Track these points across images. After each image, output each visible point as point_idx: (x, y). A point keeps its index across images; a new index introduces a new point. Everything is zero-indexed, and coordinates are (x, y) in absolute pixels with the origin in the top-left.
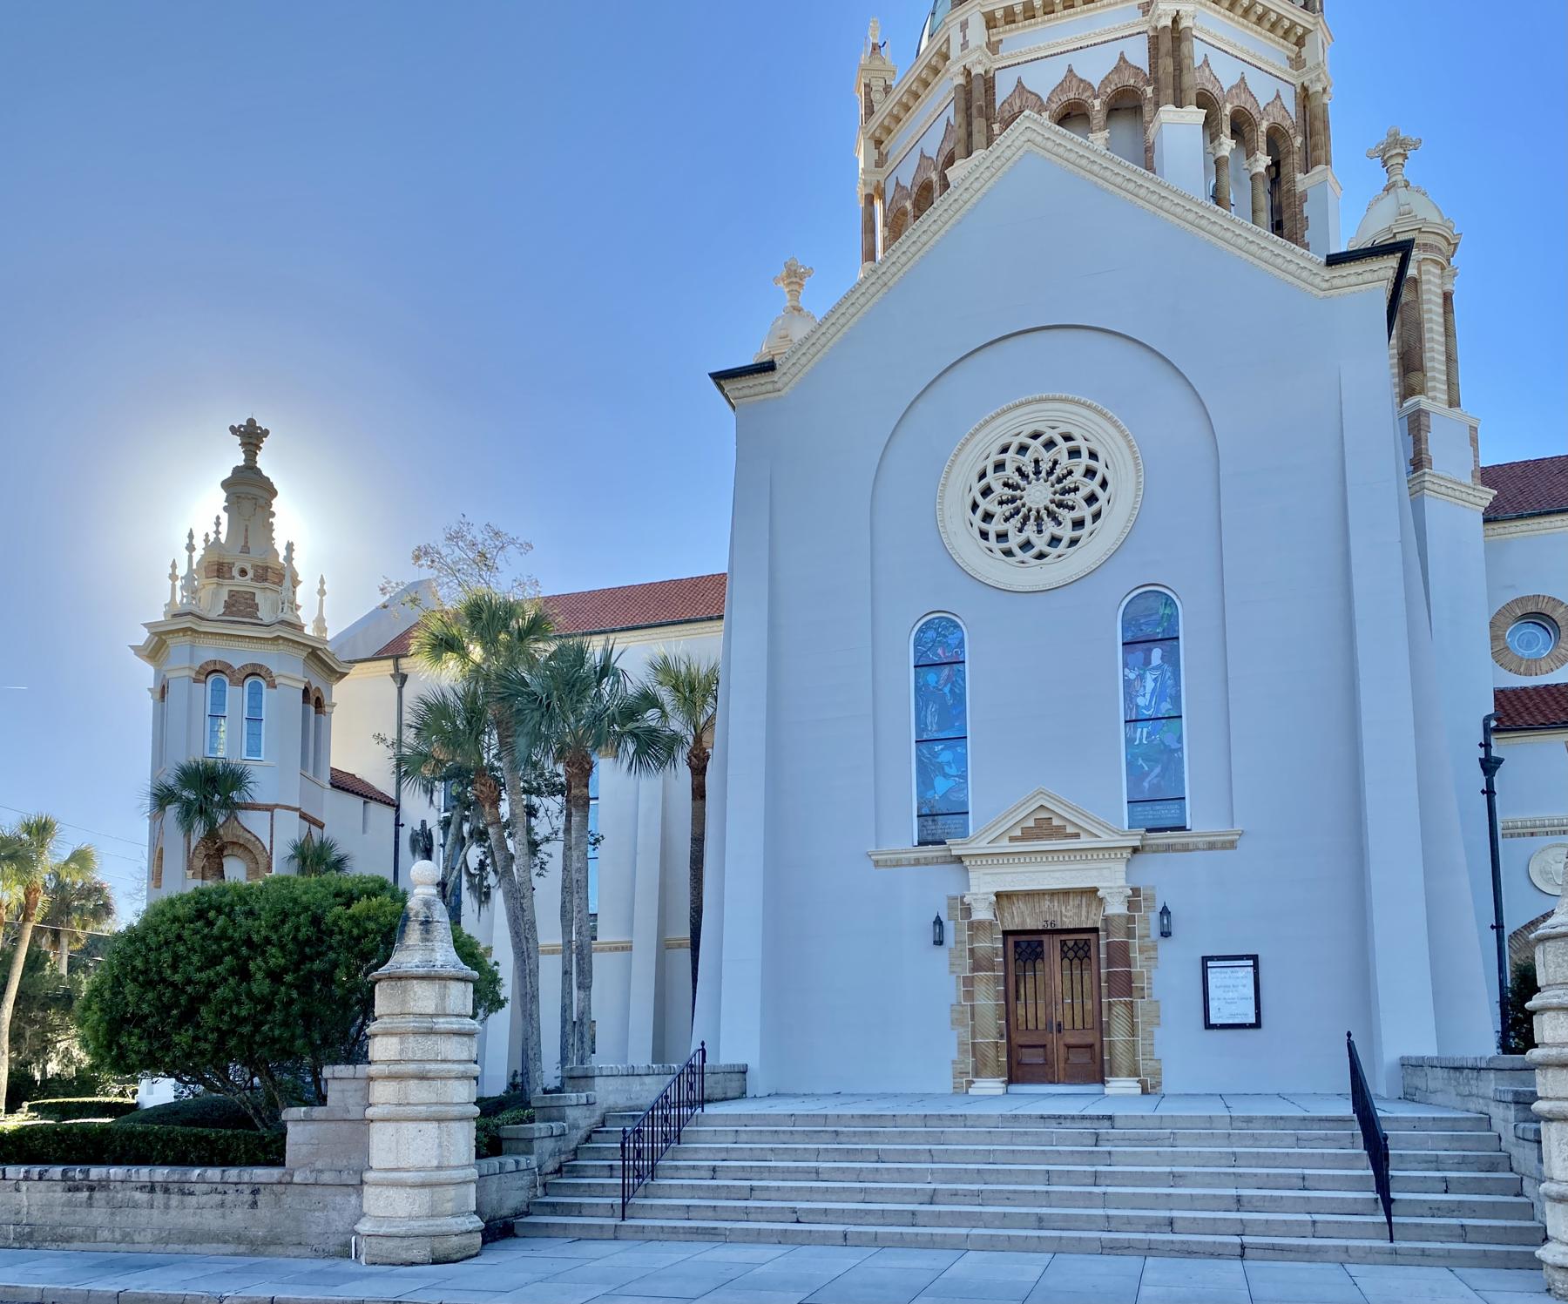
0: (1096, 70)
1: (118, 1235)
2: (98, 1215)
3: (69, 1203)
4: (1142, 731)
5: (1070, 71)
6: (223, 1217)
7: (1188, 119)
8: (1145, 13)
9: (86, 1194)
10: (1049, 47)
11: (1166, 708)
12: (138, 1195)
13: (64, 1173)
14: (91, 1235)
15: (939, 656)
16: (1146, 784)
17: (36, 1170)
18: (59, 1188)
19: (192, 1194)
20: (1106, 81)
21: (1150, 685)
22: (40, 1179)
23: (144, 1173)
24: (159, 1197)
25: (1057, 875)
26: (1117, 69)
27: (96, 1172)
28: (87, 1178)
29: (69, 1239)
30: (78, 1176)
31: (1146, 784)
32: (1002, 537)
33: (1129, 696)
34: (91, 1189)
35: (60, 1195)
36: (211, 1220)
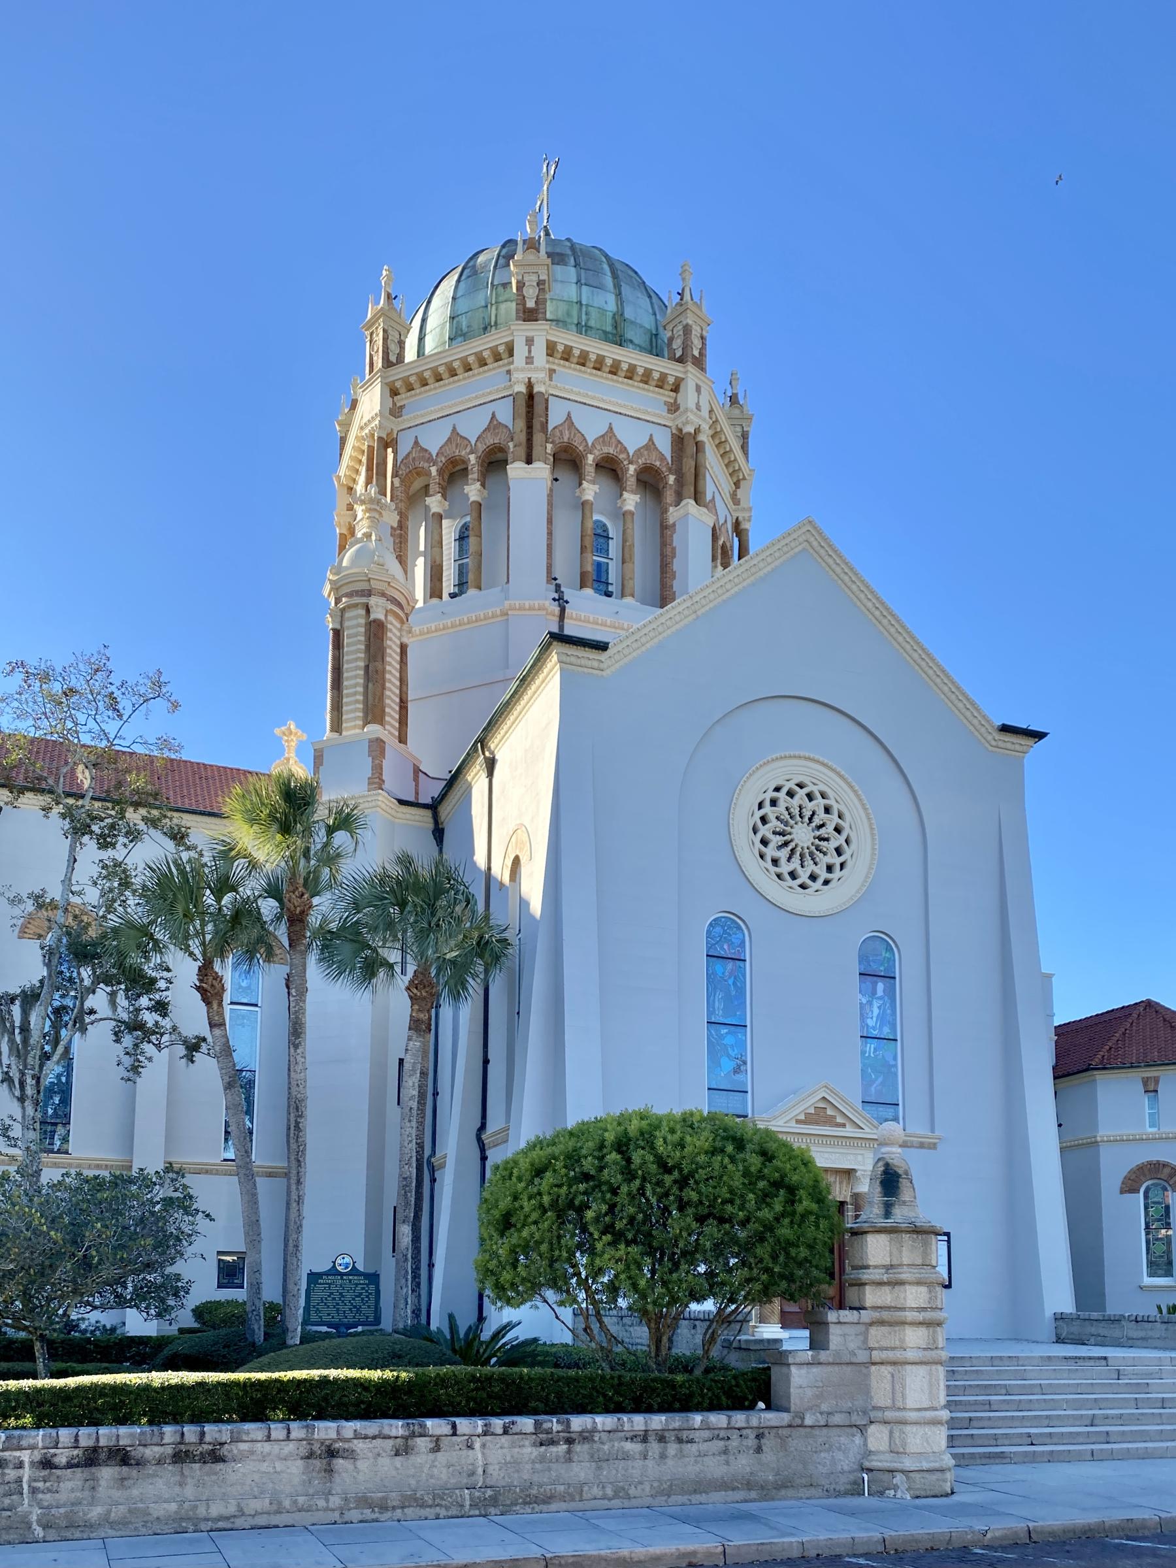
0: (632, 439)
1: (609, 1491)
2: (581, 1471)
3: (542, 1459)
4: (871, 1046)
5: (611, 428)
6: (727, 1463)
7: (704, 518)
8: (669, 411)
9: (565, 1447)
10: (593, 398)
11: (886, 1032)
12: (629, 1446)
13: (537, 1425)
14: (575, 1493)
15: (725, 952)
16: (873, 1089)
17: (498, 1423)
18: (527, 1443)
19: (691, 1441)
20: (638, 452)
21: (876, 1011)
22: (506, 1432)
23: (638, 1421)
24: (654, 1447)
25: (826, 1155)
26: (646, 447)
27: (578, 1422)
28: (567, 1429)
29: (548, 1499)
30: (556, 1427)
31: (873, 1089)
32: (830, 869)
33: (863, 1017)
34: (570, 1441)
35: (529, 1451)
36: (714, 1468)
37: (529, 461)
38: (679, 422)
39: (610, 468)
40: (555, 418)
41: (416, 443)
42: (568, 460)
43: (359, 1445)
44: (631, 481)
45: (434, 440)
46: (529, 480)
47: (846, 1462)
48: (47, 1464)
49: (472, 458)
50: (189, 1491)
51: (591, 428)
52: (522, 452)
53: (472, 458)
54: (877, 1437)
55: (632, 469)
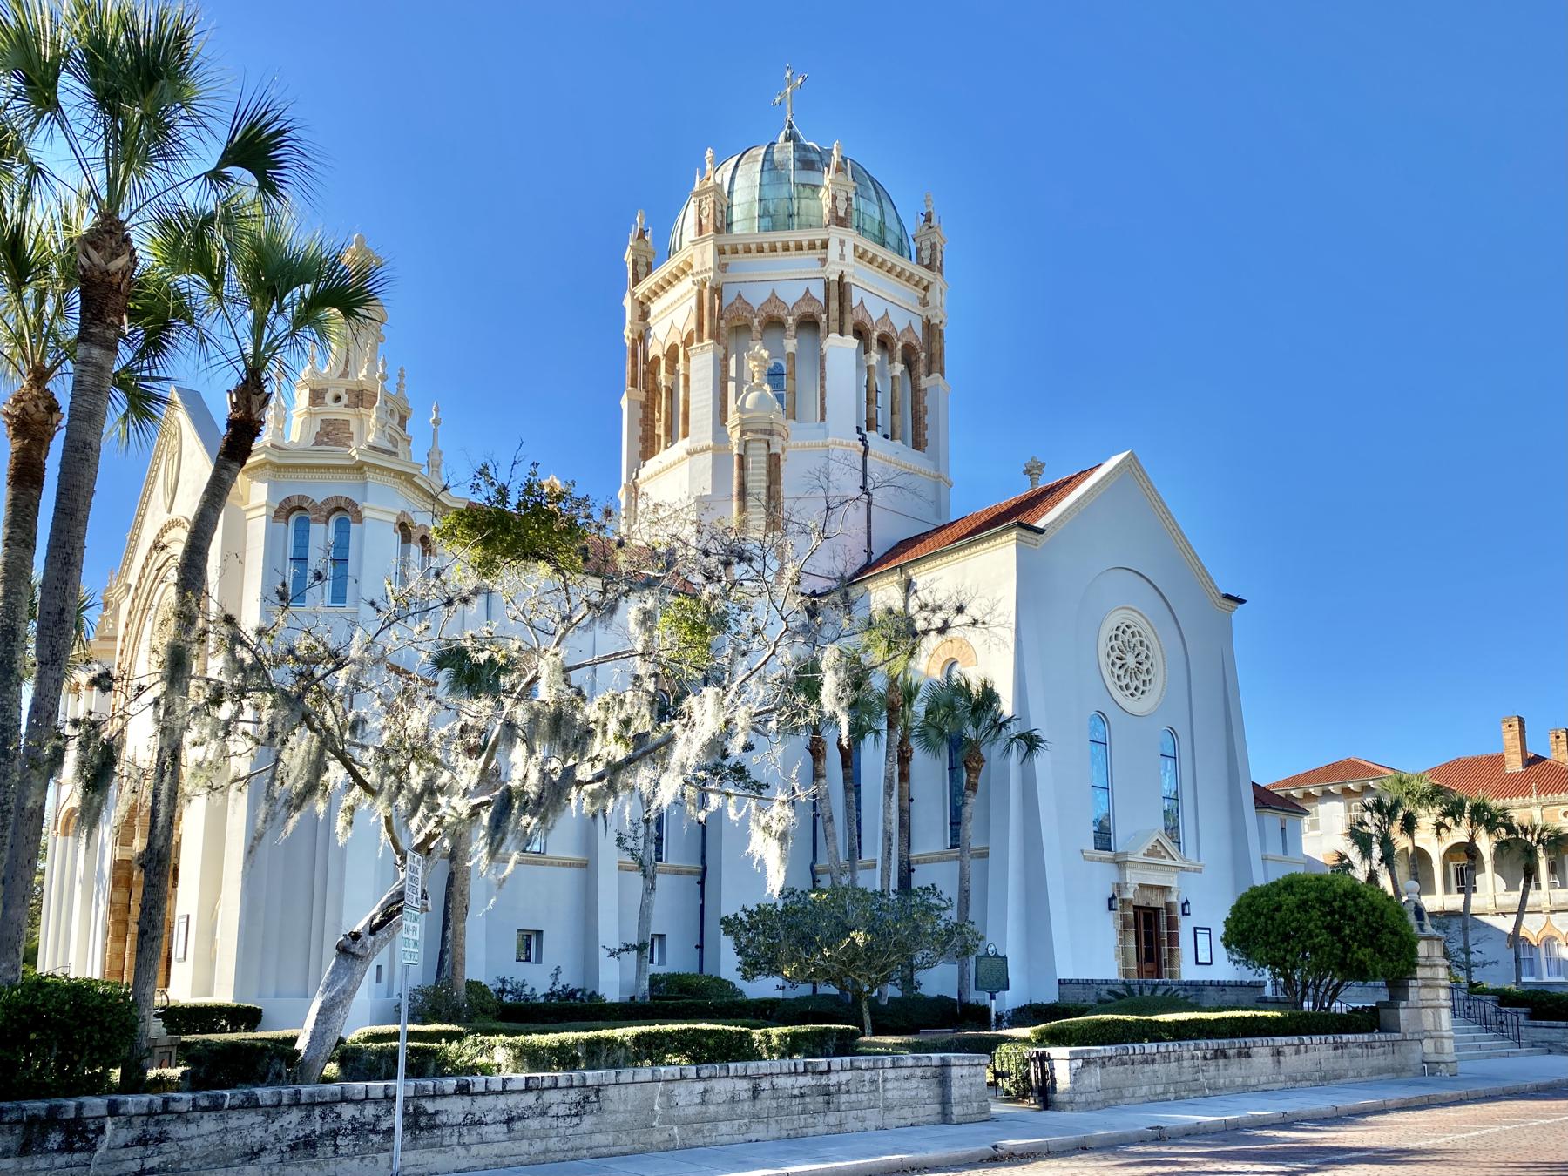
2: (1345, 1063)
27: (1345, 1037)
37: (841, 333)
38: (929, 314)
39: (884, 342)
40: (856, 297)
41: (740, 296)
42: (861, 333)
43: (1286, 1049)
44: (899, 355)
45: (757, 297)
46: (840, 349)
47: (1417, 1058)
48: (1205, 1058)
49: (790, 319)
50: (1243, 1072)
51: (875, 311)
52: (835, 325)
53: (790, 319)
54: (1428, 1046)
55: (900, 345)
